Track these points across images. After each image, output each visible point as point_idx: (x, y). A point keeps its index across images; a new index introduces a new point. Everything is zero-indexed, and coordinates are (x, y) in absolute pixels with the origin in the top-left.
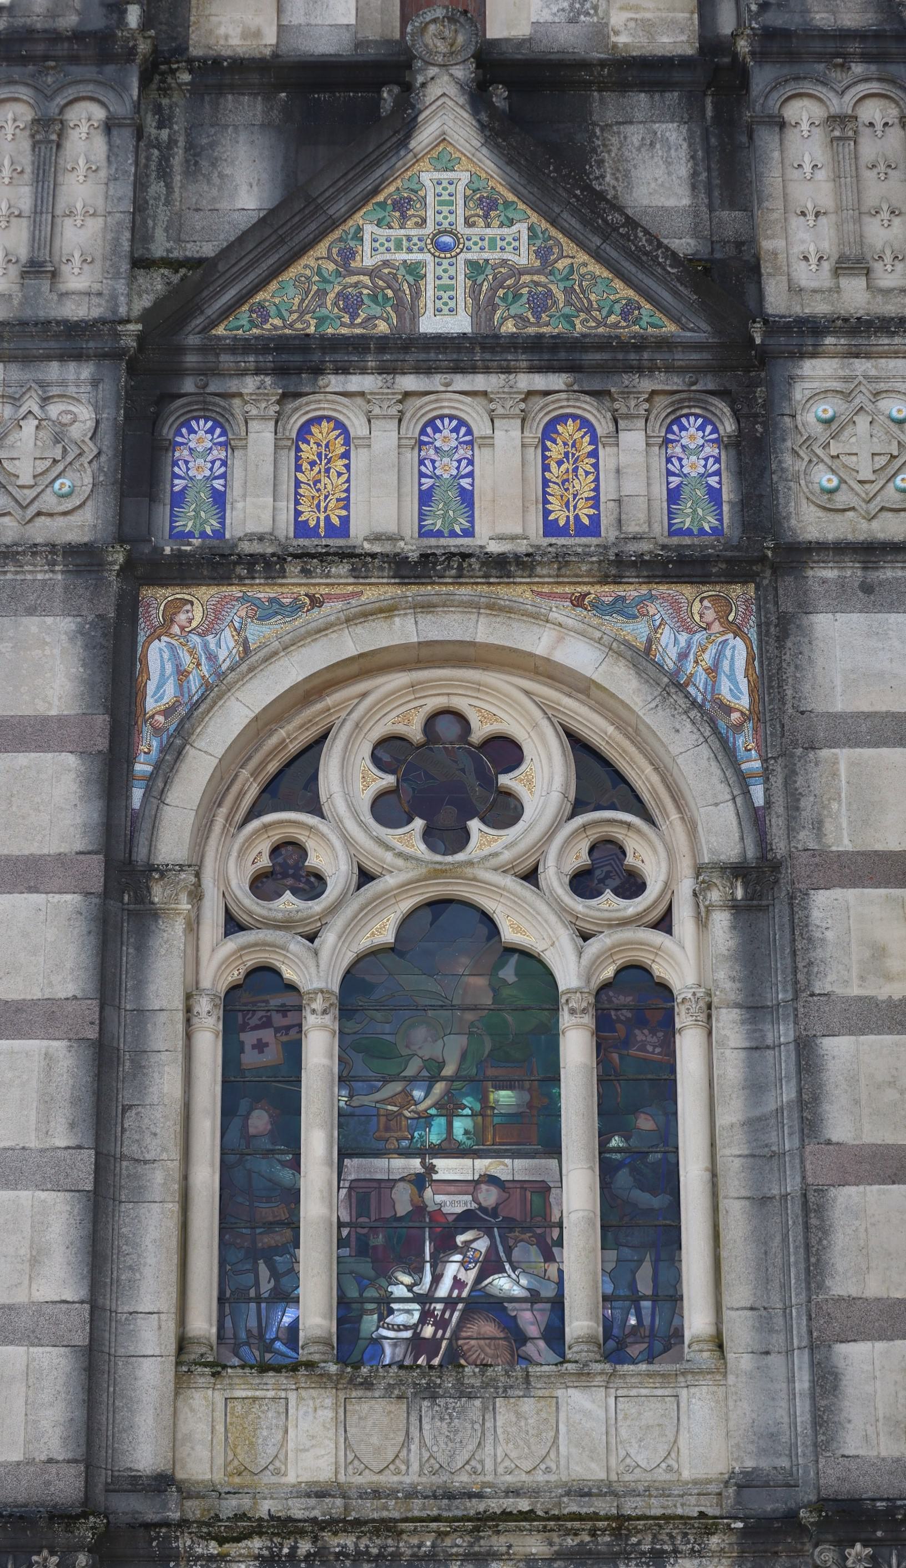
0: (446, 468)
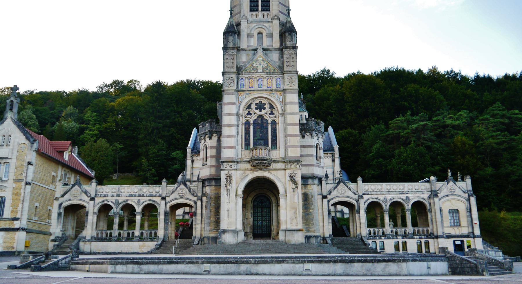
0: (260, 82)
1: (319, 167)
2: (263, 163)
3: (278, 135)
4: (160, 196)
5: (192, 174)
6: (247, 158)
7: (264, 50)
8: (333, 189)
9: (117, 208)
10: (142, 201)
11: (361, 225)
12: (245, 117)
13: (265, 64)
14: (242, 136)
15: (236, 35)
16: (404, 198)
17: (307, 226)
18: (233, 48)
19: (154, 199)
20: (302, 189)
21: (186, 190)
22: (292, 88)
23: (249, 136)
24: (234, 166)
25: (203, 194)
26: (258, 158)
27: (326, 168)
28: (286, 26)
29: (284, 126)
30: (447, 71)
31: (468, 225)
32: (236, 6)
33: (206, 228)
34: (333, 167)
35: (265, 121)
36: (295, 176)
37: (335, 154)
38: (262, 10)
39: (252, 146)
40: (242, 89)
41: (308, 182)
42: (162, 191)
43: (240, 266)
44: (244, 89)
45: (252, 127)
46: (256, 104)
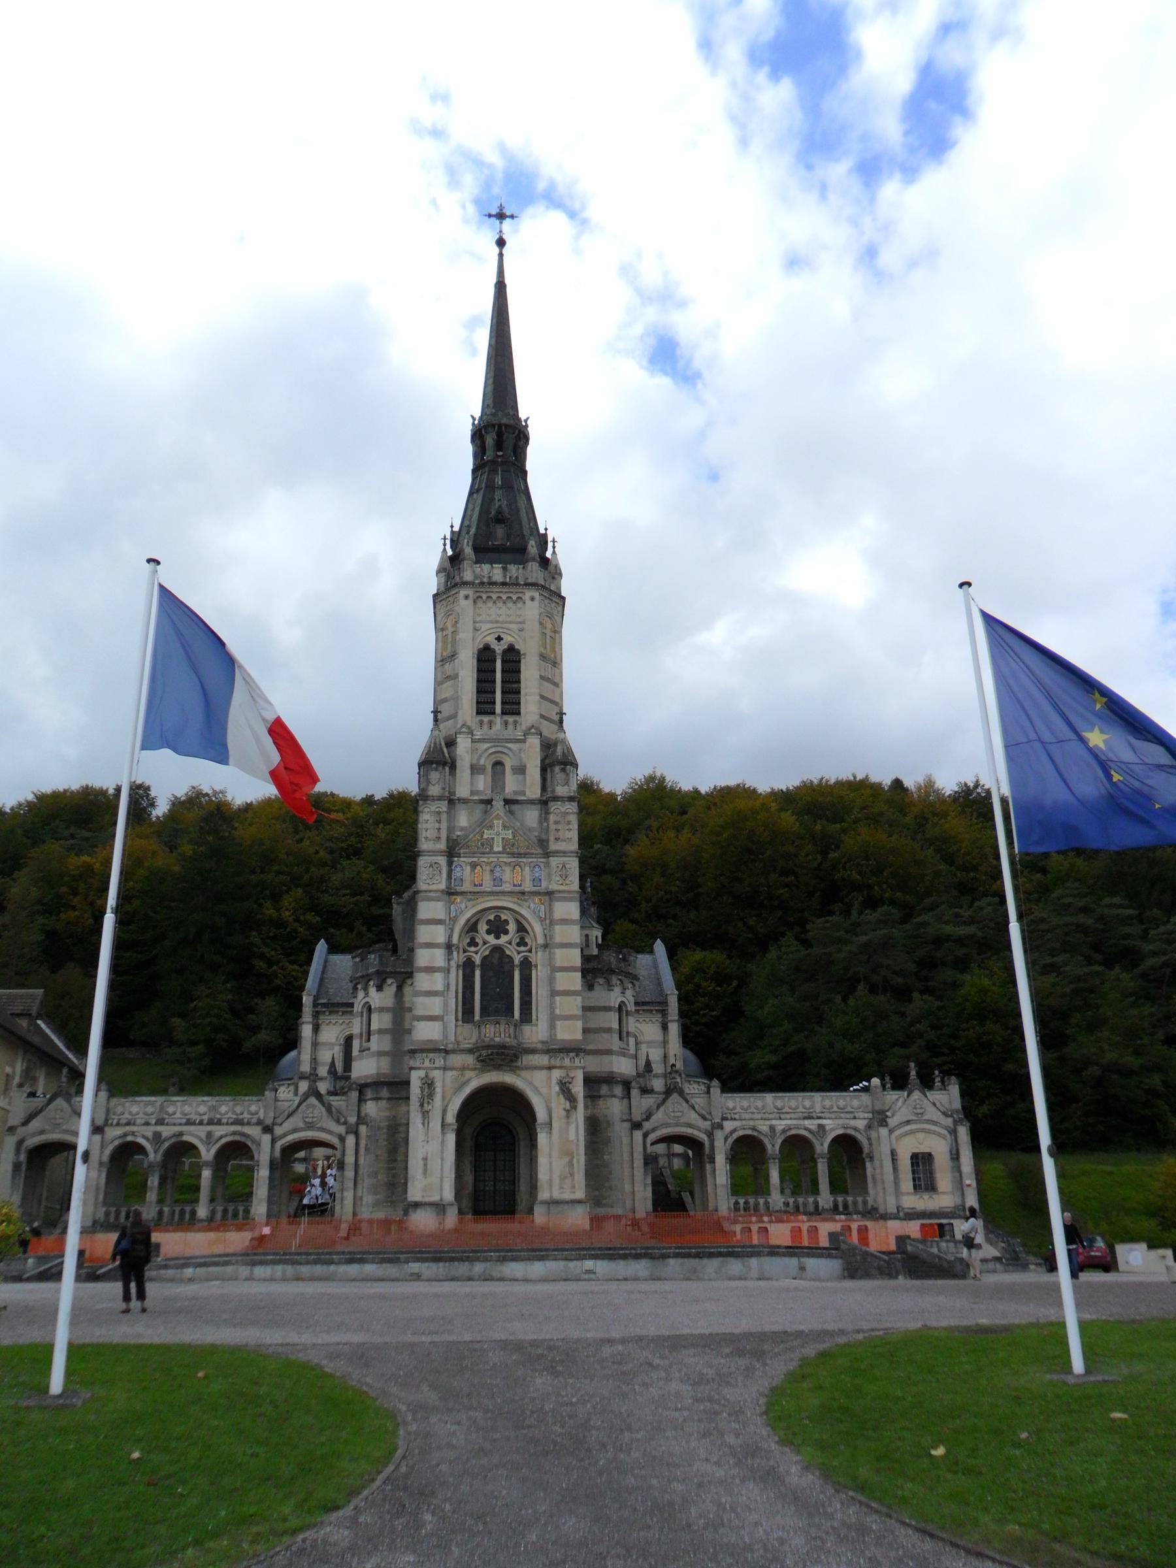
0: (497, 874)
1: (624, 1056)
2: (503, 1054)
3: (534, 991)
4: (259, 1122)
5: (315, 1059)
6: (467, 1041)
7: (507, 802)
8: (655, 1107)
9: (156, 1152)
10: (218, 1134)
11: (719, 1190)
12: (465, 951)
13: (509, 834)
14: (457, 992)
15: (447, 769)
16: (813, 1128)
17: (597, 1193)
18: (440, 798)
19: (247, 1130)
20: (586, 1107)
21: (320, 1110)
22: (566, 888)
23: (473, 994)
24: (440, 1062)
25: (361, 1120)
26: (492, 1043)
27: (648, 1047)
28: (555, 751)
29: (549, 972)
30: (963, 782)
31: (953, 1188)
32: (445, 700)
33: (365, 1199)
34: (665, 1042)
35: (507, 960)
36: (570, 1083)
37: (670, 1011)
38: (504, 713)
39: (477, 1017)
40: (459, 889)
41: (599, 1091)
42: (265, 1111)
43: (472, 1265)
44: (463, 889)
45: (478, 973)
46: (489, 922)
